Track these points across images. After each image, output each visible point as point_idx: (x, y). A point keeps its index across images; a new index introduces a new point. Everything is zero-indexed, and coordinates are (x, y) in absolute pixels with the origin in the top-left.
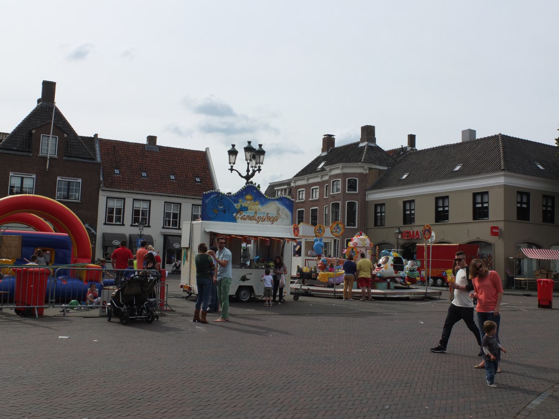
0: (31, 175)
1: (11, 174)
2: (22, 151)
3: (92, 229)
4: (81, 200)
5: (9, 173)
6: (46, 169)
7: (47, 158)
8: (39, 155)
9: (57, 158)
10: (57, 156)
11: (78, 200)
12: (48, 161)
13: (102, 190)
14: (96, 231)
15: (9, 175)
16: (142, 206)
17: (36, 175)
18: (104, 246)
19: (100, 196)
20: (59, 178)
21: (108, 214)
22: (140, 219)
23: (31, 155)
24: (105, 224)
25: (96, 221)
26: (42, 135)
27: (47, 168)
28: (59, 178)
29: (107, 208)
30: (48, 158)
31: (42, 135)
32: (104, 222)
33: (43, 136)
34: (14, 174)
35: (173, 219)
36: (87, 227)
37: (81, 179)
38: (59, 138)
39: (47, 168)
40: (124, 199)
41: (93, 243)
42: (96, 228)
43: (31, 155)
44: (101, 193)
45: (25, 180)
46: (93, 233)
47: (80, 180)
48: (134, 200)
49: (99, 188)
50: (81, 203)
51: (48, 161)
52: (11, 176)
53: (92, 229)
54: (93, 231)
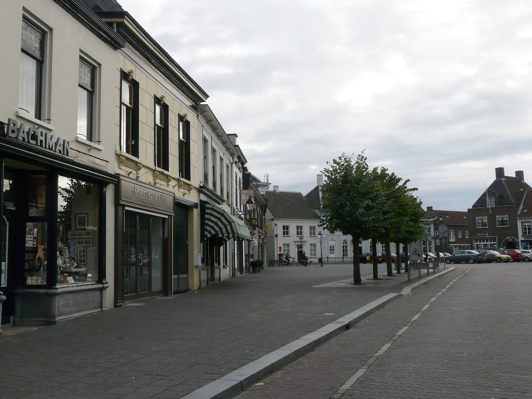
1: (477, 218)
2: (481, 207)
8: (487, 207)
14: (518, 240)
20: (497, 217)
23: (483, 208)
27: (491, 213)
28: (497, 217)
39: (491, 213)
43: (483, 208)
44: (518, 221)
45: (483, 219)
46: (517, 241)
47: (507, 216)
52: (477, 219)
53: (516, 239)
54: (517, 240)
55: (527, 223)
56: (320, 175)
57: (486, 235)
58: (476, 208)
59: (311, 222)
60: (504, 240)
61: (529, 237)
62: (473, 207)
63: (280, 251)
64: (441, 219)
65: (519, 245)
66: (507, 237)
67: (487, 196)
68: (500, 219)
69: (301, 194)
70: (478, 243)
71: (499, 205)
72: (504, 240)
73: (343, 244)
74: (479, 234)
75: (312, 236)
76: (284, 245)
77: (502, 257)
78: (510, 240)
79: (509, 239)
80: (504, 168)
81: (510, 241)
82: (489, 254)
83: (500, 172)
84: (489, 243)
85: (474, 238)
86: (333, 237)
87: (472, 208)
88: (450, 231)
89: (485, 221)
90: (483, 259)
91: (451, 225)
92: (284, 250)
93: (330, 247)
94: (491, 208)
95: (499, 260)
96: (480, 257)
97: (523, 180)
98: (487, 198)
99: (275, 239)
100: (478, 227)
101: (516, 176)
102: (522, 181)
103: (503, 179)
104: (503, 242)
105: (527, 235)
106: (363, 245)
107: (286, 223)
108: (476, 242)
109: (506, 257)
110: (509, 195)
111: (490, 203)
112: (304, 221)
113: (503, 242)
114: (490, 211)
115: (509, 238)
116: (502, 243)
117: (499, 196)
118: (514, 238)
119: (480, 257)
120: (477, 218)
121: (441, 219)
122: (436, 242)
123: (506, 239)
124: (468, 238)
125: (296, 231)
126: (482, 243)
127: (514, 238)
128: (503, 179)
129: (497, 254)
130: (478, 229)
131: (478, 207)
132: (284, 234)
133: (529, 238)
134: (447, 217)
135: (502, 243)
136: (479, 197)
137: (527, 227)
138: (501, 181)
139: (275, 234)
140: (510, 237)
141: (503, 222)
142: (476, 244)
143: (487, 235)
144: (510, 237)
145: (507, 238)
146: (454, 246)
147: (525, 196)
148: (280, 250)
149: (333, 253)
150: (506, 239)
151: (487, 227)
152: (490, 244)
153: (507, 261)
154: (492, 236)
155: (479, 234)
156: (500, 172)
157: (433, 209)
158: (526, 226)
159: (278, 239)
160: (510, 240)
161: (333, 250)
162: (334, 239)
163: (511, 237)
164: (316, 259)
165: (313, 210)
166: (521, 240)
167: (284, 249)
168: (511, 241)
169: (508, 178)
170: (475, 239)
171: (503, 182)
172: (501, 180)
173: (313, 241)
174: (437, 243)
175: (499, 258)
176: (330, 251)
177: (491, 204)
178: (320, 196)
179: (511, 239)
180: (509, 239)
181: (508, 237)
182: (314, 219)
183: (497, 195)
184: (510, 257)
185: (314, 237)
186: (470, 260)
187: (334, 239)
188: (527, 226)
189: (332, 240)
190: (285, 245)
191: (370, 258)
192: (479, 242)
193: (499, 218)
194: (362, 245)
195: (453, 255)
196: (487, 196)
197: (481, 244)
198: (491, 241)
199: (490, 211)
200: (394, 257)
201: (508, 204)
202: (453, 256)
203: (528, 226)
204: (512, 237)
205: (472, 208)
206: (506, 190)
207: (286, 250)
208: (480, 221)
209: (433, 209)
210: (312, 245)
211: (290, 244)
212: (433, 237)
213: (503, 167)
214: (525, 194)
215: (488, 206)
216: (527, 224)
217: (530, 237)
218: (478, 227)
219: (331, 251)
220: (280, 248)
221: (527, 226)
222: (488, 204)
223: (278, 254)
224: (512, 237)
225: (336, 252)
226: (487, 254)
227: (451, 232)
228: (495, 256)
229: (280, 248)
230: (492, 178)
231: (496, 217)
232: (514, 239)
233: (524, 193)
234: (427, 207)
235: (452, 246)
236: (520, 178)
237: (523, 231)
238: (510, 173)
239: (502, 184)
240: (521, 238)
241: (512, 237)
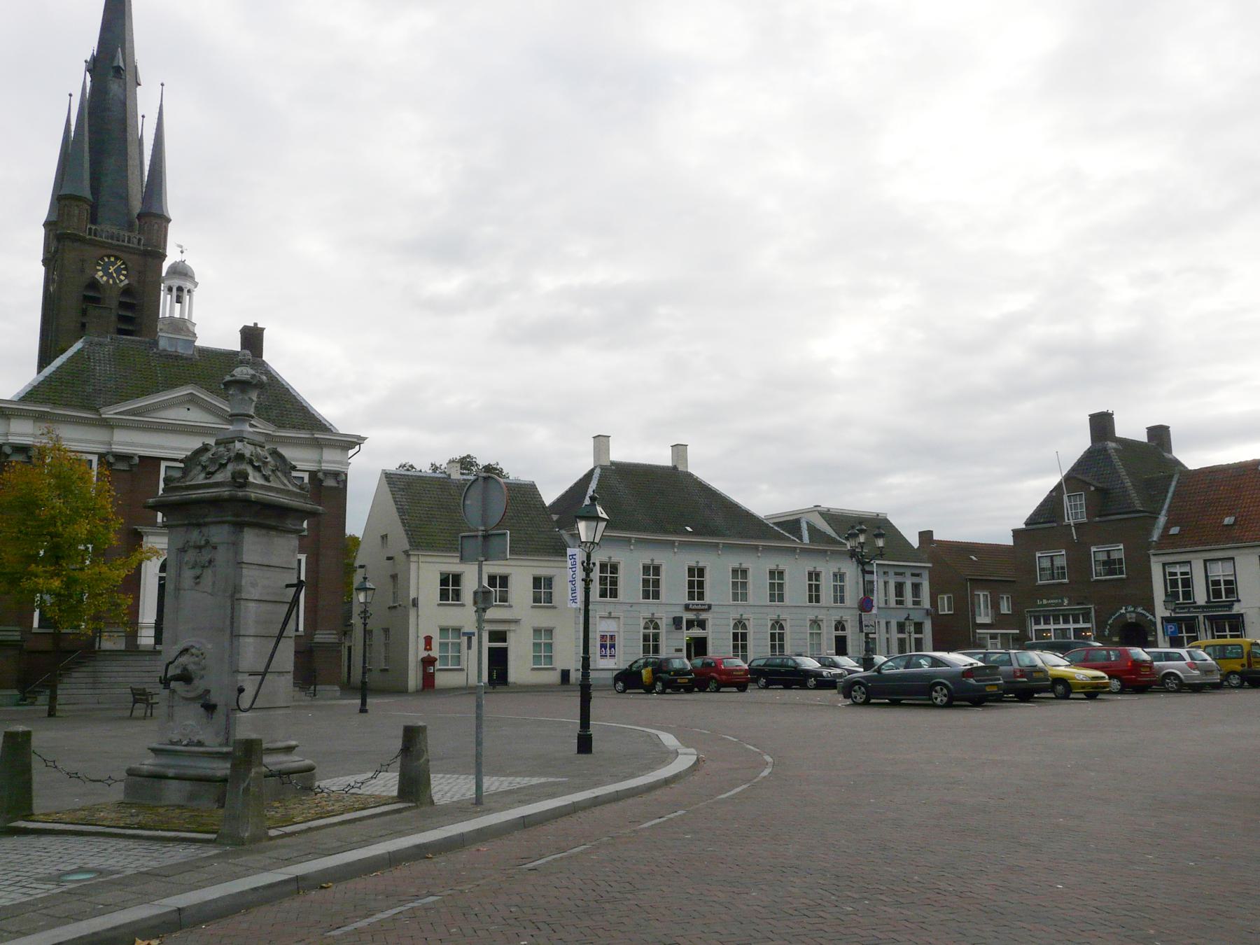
1: (1038, 555)
2: (1049, 522)
3: (1148, 614)
6: (1074, 540)
7: (1070, 525)
12: (1073, 528)
13: (1154, 555)
14: (1155, 617)
16: (1220, 571)
19: (1152, 564)
20: (1093, 549)
21: (1212, 586)
22: (1181, 593)
23: (1055, 525)
27: (1075, 538)
28: (1093, 549)
29: (1168, 581)
30: (1072, 524)
34: (1041, 553)
35: (1178, 591)
36: (1141, 611)
39: (1075, 538)
40: (1233, 559)
43: (1055, 525)
44: (1153, 559)
45: (1054, 558)
48: (1205, 561)
50: (1128, 578)
51: (1073, 528)
52: (1039, 557)
53: (1148, 614)
54: (1151, 617)
55: (1180, 566)
56: (600, 437)
57: (1063, 602)
58: (1034, 527)
59: (546, 564)
60: (1113, 617)
61: (1183, 608)
62: (1026, 524)
63: (426, 649)
64: (880, 543)
65: (1156, 632)
66: (1122, 609)
67: (1065, 492)
68: (1103, 557)
69: (535, 485)
70: (1042, 627)
71: (1100, 516)
72: (1113, 617)
73: (645, 628)
74: (1045, 602)
75: (542, 604)
76: (444, 630)
77: (1075, 678)
78: (1130, 618)
79: (1129, 613)
80: (1113, 414)
81: (1129, 621)
82: (1018, 667)
83: (1101, 424)
84: (1072, 626)
85: (1030, 612)
86: (610, 608)
87: (1024, 526)
88: (979, 595)
89: (1061, 561)
90: (988, 689)
91: (982, 580)
92: (443, 646)
93: (603, 637)
94: (1075, 524)
95: (1060, 688)
96: (972, 681)
97: (1170, 451)
98: (1065, 497)
99: (412, 612)
100: (1041, 580)
101: (1148, 440)
102: (1165, 454)
103: (1111, 445)
104: (1109, 622)
105: (1181, 601)
106: (710, 634)
107: (452, 565)
108: (1035, 624)
109: (1086, 676)
110: (1126, 487)
111: (1074, 512)
112: (536, 562)
113: (1109, 622)
114: (1074, 531)
115: (1126, 612)
116: (1108, 627)
117: (1097, 489)
118: (1143, 612)
119: (972, 681)
120: (1038, 555)
121: (880, 543)
122: (861, 622)
124: (1010, 612)
125: (439, 587)
126: (1052, 627)
127: (1143, 612)
128: (1111, 445)
129: (1056, 664)
130: (1039, 586)
131: (1040, 523)
132: (537, 599)
133: (1186, 610)
134: (973, 557)
135: (1108, 627)
136: (1045, 496)
137: (1179, 576)
138: (1105, 449)
139: (412, 595)
140: (1131, 609)
141: (1110, 566)
142: (1035, 630)
143: (1066, 602)
144: (1129, 609)
145: (1123, 611)
146: (990, 633)
147: (1172, 489)
148: (426, 645)
149: (612, 656)
151: (1066, 581)
152: (1074, 629)
153: (1093, 692)
154: (1078, 604)
155: (1045, 602)
156: (1101, 424)
157: (935, 538)
158: (1175, 574)
159: (420, 613)
160: (1131, 618)
161: (612, 646)
162: (613, 615)
163: (1133, 609)
164: (551, 672)
165: (557, 530)
166: (1162, 618)
167: (441, 644)
168: (1134, 621)
169: (1128, 445)
170: (1032, 614)
171: (1110, 451)
172: (1105, 448)
173: (543, 618)
174: (864, 623)
175: (1061, 680)
176: (601, 651)
177: (1077, 513)
178: (588, 493)
179: (1134, 615)
180: (1128, 615)
181: (1126, 609)
182: (549, 554)
183: (1093, 486)
184: (1103, 678)
185: (547, 607)
186: (936, 692)
187: (613, 615)
188: (1179, 574)
189: (608, 618)
190: (448, 630)
191: (651, 674)
192: (1045, 624)
193: (1098, 552)
194: (708, 633)
195: (874, 671)
196: (1065, 492)
197: (1050, 630)
198: (1076, 621)
199: (1074, 531)
200: (737, 670)
201: (1126, 513)
202: (876, 673)
203: (1182, 574)
205: (1024, 526)
206: (1117, 472)
207: (450, 644)
208: (1046, 564)
209: (935, 538)
210: (540, 631)
211: (554, 628)
212: (927, 610)
213: (1110, 412)
214: (1174, 484)
215: (1069, 519)
216: (1178, 569)
217: (1189, 608)
218: (1041, 580)
219: (605, 649)
220: (428, 640)
221: (1179, 574)
222: (1068, 513)
223: (420, 658)
225: (622, 652)
226: (1012, 665)
227: (981, 596)
228: (1041, 675)
229: (428, 640)
230: (1081, 442)
231: (1090, 550)
232: (1141, 613)
233: (1171, 481)
234: (920, 533)
235: (985, 636)
236: (1158, 444)
237: (1169, 590)
238: (1130, 427)
239: (1108, 457)
240: (1161, 611)
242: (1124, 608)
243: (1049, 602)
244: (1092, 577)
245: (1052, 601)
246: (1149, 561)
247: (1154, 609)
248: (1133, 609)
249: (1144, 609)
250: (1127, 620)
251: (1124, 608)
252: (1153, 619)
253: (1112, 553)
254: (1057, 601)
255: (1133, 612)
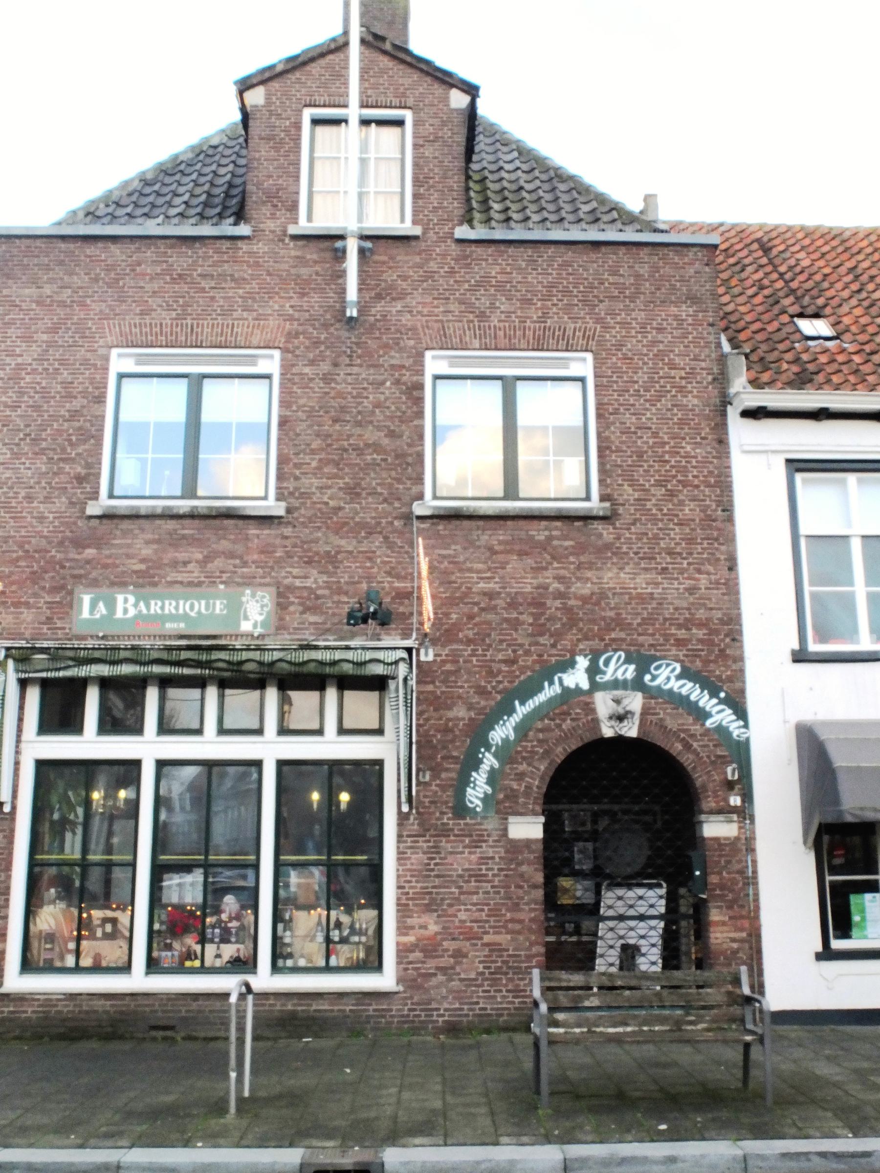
0: (252, 360)
3: (706, 702)
4: (603, 499)
5: (107, 359)
8: (292, 230)
9: (417, 231)
10: (415, 222)
11: (588, 498)
14: (741, 713)
15: (106, 369)
17: (285, 350)
18: (824, 829)
24: (800, 657)
25: (735, 636)
26: (308, 114)
27: (352, 293)
29: (803, 542)
31: (308, 114)
32: (796, 646)
33: (316, 122)
36: (675, 685)
37: (589, 356)
38: (416, 124)
39: (352, 293)
41: (734, 810)
42: (742, 692)
46: (722, 730)
49: (725, 401)
52: (121, 376)
53: (706, 702)
55: (860, 481)
57: (236, 610)
60: (521, 711)
65: (747, 796)
66: (571, 664)
72: (521, 711)
81: (608, 732)
108: (46, 727)
115: (595, 686)
116: (489, 761)
118: (688, 689)
123: (549, 692)
127: (688, 689)
142: (42, 765)
150: (549, 692)
152: (282, 764)
179: (635, 702)
180: (603, 704)
181: (593, 671)
197: (135, 765)
204: (643, 669)
224: (643, 663)
241: (643, 663)
242: (582, 662)
243: (155, 607)
244: (420, 497)
245: (170, 607)
246: (722, 442)
247: (739, 675)
248: (630, 672)
249: (686, 674)
250: (596, 722)
251: (582, 662)
252: (735, 729)
253: (523, 390)
254: (201, 606)
255: (638, 684)
